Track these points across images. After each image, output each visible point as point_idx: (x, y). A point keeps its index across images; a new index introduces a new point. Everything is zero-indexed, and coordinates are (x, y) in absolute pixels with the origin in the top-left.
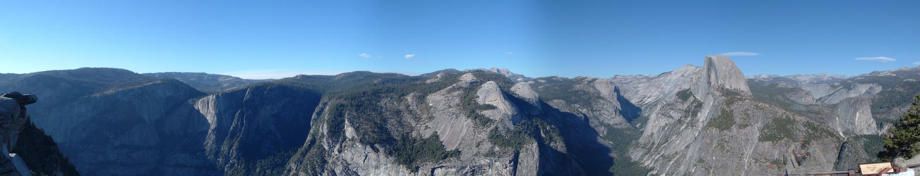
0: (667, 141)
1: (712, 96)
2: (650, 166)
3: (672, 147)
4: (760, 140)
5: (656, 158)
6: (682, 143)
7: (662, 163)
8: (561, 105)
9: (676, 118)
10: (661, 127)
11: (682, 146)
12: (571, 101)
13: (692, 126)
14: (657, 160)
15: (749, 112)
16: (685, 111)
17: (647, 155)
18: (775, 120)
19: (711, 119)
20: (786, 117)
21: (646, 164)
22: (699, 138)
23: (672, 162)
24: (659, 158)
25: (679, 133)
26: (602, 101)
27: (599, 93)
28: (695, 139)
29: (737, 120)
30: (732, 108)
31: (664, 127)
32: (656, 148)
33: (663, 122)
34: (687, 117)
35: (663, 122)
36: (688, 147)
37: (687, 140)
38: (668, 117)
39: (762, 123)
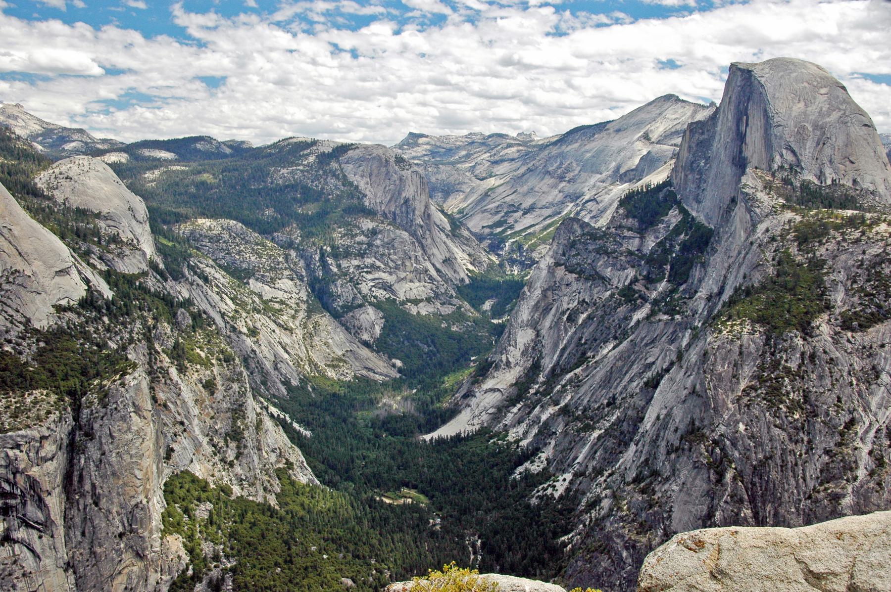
0: (582, 359)
1: (749, 210)
2: (524, 443)
5: (544, 417)
6: (636, 369)
7: (565, 433)
9: (615, 281)
10: (563, 313)
11: (631, 381)
13: (671, 312)
14: (546, 423)
16: (650, 260)
17: (515, 406)
19: (736, 290)
21: (511, 437)
22: (693, 356)
23: (596, 434)
24: (553, 417)
25: (625, 335)
28: (680, 356)
29: (838, 297)
30: (821, 252)
36: (653, 384)
37: (650, 360)
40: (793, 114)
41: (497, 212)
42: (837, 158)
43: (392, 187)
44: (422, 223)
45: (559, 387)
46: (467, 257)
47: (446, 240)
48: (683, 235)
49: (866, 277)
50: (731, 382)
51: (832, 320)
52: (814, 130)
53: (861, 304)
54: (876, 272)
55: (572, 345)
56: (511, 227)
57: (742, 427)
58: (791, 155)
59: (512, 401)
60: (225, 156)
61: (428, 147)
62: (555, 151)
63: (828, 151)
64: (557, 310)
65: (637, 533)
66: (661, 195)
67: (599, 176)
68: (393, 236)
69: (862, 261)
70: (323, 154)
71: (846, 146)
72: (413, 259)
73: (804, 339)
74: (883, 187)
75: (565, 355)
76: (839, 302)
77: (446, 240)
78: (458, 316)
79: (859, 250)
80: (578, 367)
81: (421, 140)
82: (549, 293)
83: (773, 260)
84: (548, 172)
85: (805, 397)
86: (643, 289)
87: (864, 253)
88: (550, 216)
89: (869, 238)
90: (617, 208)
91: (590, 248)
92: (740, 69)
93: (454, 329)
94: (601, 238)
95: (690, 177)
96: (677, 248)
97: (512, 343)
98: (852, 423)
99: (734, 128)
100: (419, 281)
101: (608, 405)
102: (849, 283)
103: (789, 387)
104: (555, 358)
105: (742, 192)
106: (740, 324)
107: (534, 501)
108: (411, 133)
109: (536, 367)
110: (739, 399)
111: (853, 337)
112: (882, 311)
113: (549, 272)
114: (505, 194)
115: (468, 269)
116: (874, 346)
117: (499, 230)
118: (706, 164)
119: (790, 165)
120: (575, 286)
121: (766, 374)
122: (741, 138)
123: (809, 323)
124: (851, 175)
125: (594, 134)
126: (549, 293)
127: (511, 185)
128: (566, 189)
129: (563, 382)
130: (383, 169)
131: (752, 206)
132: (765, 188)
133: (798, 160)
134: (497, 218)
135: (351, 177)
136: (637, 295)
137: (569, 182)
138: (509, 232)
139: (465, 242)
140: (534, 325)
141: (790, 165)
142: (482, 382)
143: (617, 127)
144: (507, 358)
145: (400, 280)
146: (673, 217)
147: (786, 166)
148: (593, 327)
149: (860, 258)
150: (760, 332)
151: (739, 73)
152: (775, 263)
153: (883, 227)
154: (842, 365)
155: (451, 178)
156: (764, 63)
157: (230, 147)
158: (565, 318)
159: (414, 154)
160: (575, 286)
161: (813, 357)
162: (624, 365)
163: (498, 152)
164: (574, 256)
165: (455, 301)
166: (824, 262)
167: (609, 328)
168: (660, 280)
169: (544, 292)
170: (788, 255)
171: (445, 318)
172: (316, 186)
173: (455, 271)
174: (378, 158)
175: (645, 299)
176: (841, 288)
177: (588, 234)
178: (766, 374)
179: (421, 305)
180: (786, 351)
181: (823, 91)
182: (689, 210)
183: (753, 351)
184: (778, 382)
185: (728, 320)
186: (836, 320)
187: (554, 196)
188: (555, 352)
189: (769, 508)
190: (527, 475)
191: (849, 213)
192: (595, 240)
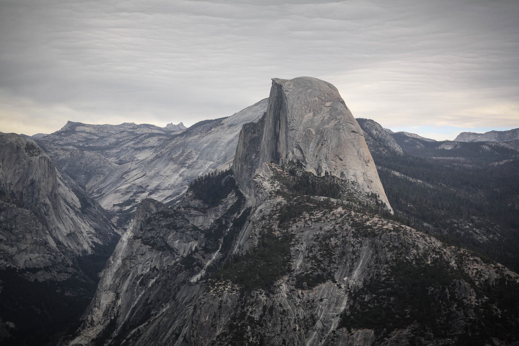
9: (181, 252)
15: (333, 241)
16: (208, 234)
20: (435, 261)
29: (298, 264)
31: (148, 277)
38: (159, 249)
39: (363, 271)
40: (305, 121)
41: (127, 193)
42: (331, 156)
43: (21, 170)
44: (48, 201)
45: (125, 341)
46: (93, 231)
47: (75, 217)
48: (235, 215)
49: (319, 248)
50: (209, 330)
51: (290, 281)
52: (316, 133)
53: (311, 268)
54: (326, 244)
55: (141, 306)
58: (300, 153)
61: (84, 135)
62: (179, 141)
63: (324, 150)
64: (133, 276)
66: (223, 181)
67: (212, 163)
68: (15, 213)
69: (318, 236)
71: (337, 147)
72: (34, 232)
73: (268, 295)
74: (362, 179)
75: (135, 314)
76: (298, 268)
77: (75, 217)
79: (318, 227)
80: (142, 324)
81: (78, 129)
82: (128, 262)
83: (260, 234)
84: (171, 159)
85: (262, 340)
86: (201, 258)
87: (321, 229)
88: (170, 196)
89: (327, 218)
90: (187, 191)
91: (163, 223)
92: (276, 84)
93: (67, 294)
94: (171, 216)
95: (245, 167)
96: (231, 224)
97: (97, 304)
99: (273, 129)
100: (39, 253)
102: (307, 251)
103: (250, 333)
104: (127, 317)
105: (254, 182)
106: (224, 285)
108: (69, 122)
109: (113, 324)
111: (302, 294)
112: (325, 274)
113: (128, 244)
114: (136, 177)
115: (93, 242)
116: (315, 301)
117: (128, 208)
118: (256, 157)
119: (298, 161)
120: (148, 256)
121: (235, 323)
123: (272, 283)
124: (340, 169)
125: (211, 128)
126: (128, 262)
127: (142, 169)
128: (185, 174)
129: (129, 336)
130: (14, 155)
131: (258, 191)
132: (272, 178)
133: (304, 156)
134: (127, 197)
136: (195, 263)
137: (188, 167)
139: (94, 217)
140: (116, 289)
141: (298, 160)
142: (73, 338)
143: (230, 123)
144: (92, 318)
145: (20, 251)
146: (231, 199)
147: (295, 161)
148: (158, 290)
149: (317, 233)
150: (237, 290)
151: (276, 87)
152: (260, 236)
153: (340, 209)
154: (291, 315)
155: (93, 163)
156: (291, 81)
158: (138, 283)
159: (70, 141)
160: (148, 256)
161: (272, 309)
162: (168, 321)
163: (142, 140)
164: (149, 230)
165: (70, 270)
166: (293, 236)
167: (169, 290)
168: (215, 250)
169: (124, 260)
170: (271, 230)
173: (78, 244)
174: (11, 145)
175: (201, 266)
176: (301, 256)
177: (162, 212)
178: (235, 323)
179: (39, 273)
180: (252, 305)
181: (328, 104)
182: (244, 194)
183: (229, 305)
184: (243, 329)
185: (216, 282)
186: (293, 280)
187: (175, 179)
188: (128, 311)
191: (322, 198)
192: (167, 218)
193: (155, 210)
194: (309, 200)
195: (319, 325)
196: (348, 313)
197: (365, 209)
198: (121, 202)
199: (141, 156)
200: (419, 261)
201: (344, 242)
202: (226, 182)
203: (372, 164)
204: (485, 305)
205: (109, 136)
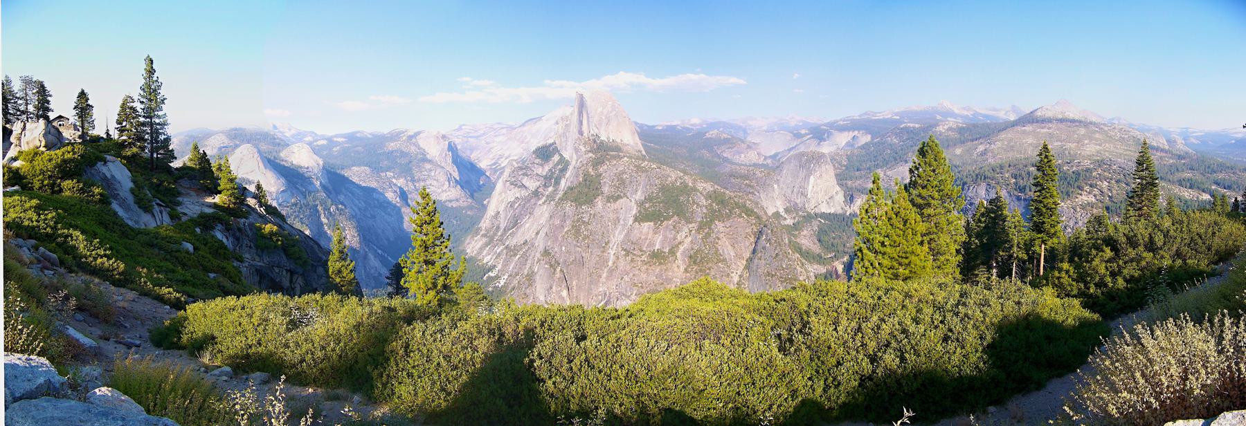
2: (489, 264)
3: (519, 234)
4: (636, 219)
5: (498, 251)
8: (363, 174)
9: (531, 188)
12: (381, 167)
14: (499, 253)
16: (546, 177)
18: (664, 189)
23: (518, 256)
24: (502, 251)
26: (428, 166)
27: (424, 153)
29: (606, 189)
31: (514, 202)
32: (501, 236)
33: (514, 194)
34: (548, 187)
35: (514, 194)
36: (537, 233)
39: (643, 192)
56: (500, 165)
57: (564, 248)
59: (486, 245)
60: (369, 139)
62: (520, 129)
65: (523, 298)
70: (410, 136)
73: (591, 208)
78: (470, 208)
81: (463, 127)
91: (520, 173)
93: (469, 213)
98: (608, 242)
101: (524, 243)
107: (490, 289)
110: (564, 236)
122: (581, 123)
134: (493, 162)
135: (421, 146)
138: (499, 167)
145: (443, 191)
146: (556, 158)
153: (625, 158)
157: (373, 135)
160: (513, 191)
165: (469, 200)
171: (464, 208)
172: (405, 150)
179: (454, 202)
189: (574, 283)
190: (489, 277)
193: (516, 166)
194: (607, 154)
195: (622, 222)
196: (638, 215)
197: (638, 158)
198: (490, 164)
199: (498, 139)
200: (673, 184)
201: (631, 176)
202: (553, 149)
203: (636, 134)
204: (711, 205)
205: (480, 130)
